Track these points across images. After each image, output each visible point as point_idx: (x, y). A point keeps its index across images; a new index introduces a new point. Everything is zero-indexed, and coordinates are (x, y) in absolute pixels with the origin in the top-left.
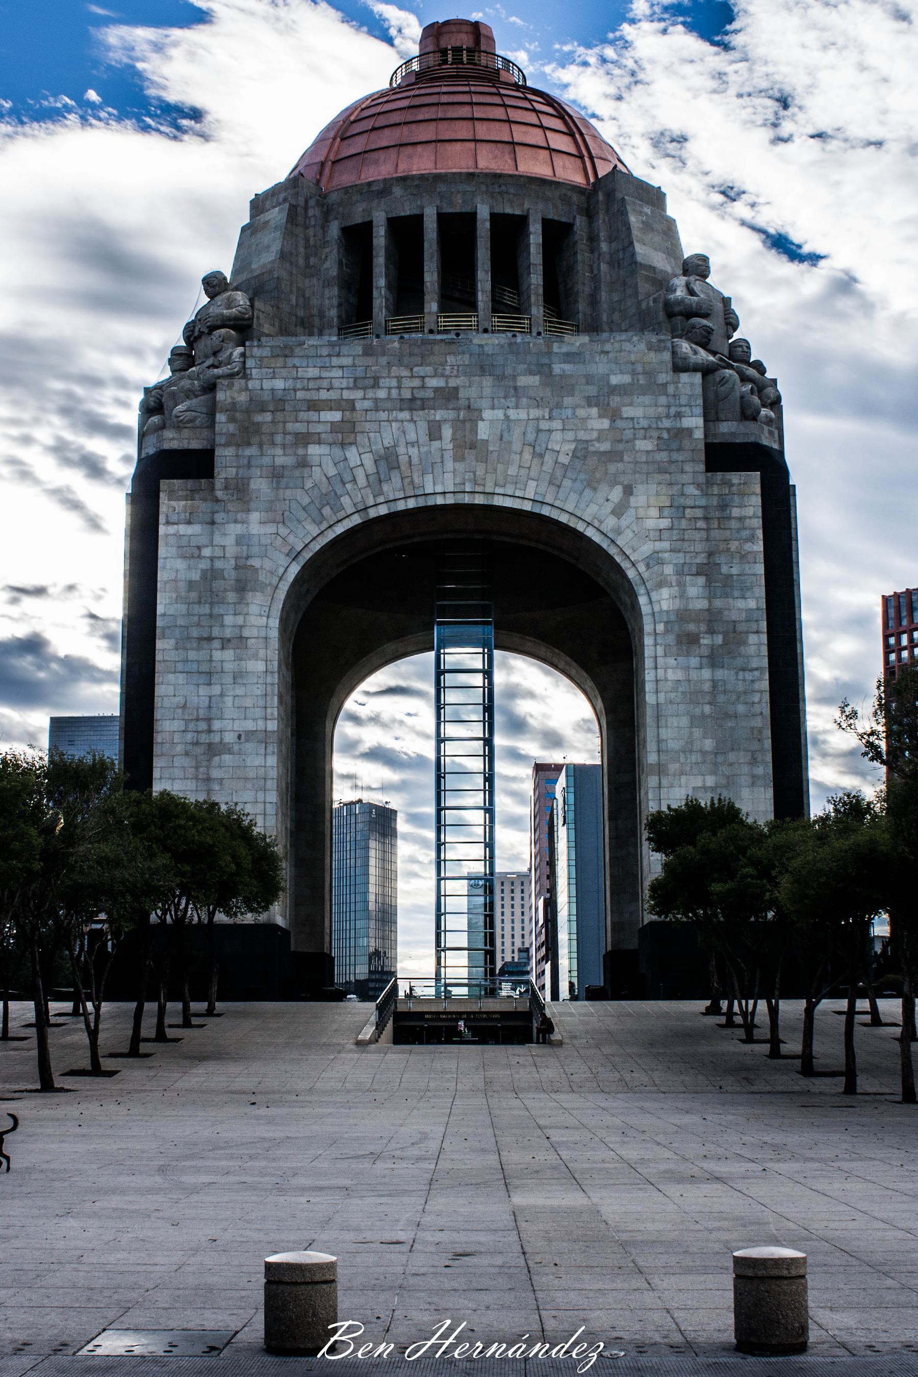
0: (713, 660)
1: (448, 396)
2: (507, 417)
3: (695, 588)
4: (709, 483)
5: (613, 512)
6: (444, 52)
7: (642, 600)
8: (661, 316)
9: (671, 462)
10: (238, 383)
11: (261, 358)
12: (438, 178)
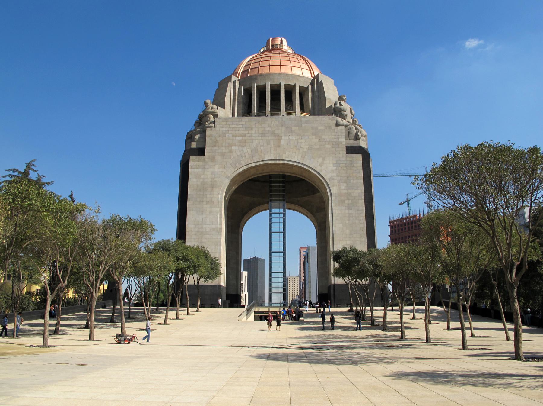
0: (349, 208)
5: (320, 165)
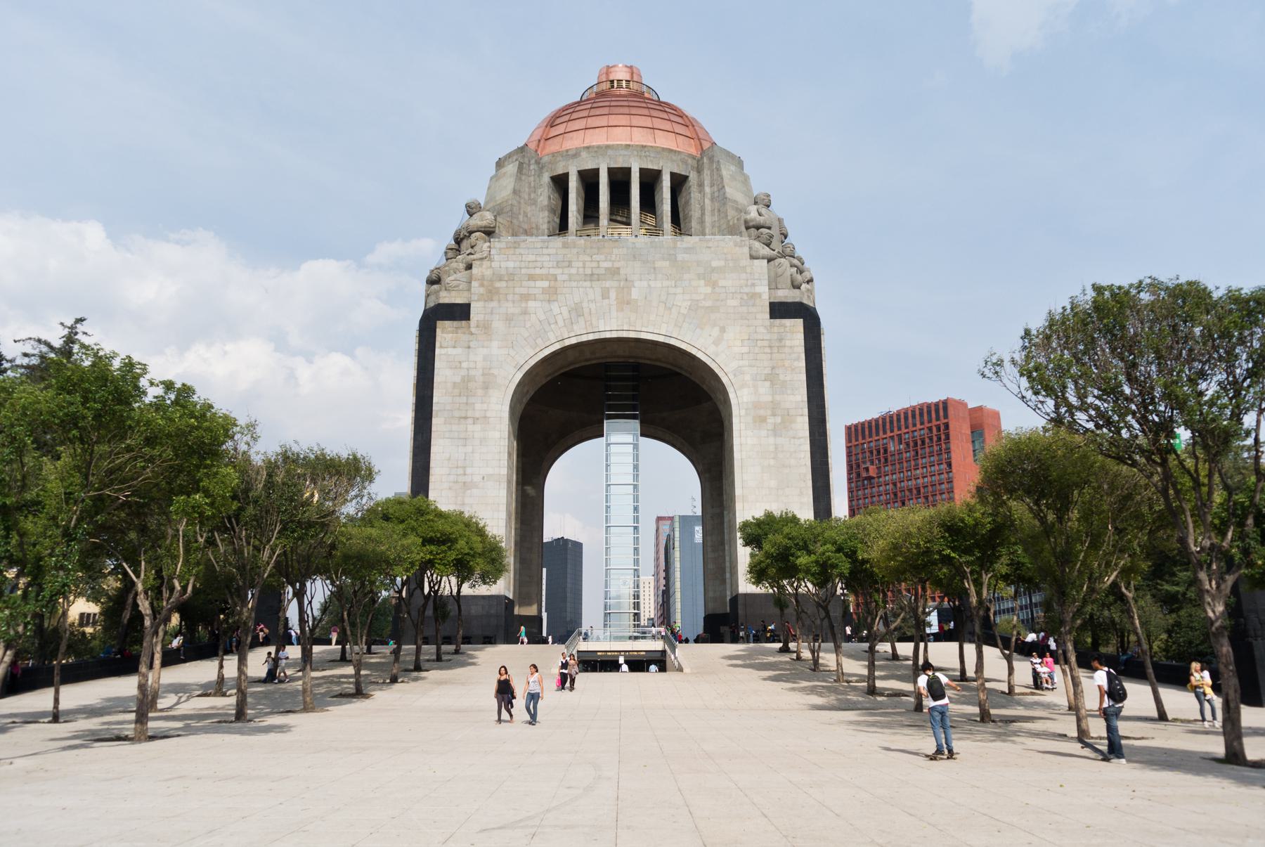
0: (775, 432)
1: (614, 272)
2: (649, 286)
3: (764, 388)
4: (772, 326)
5: (714, 343)
6: (612, 82)
7: (732, 396)
8: (743, 228)
9: (748, 313)
10: (486, 263)
11: (500, 249)
12: (608, 147)
